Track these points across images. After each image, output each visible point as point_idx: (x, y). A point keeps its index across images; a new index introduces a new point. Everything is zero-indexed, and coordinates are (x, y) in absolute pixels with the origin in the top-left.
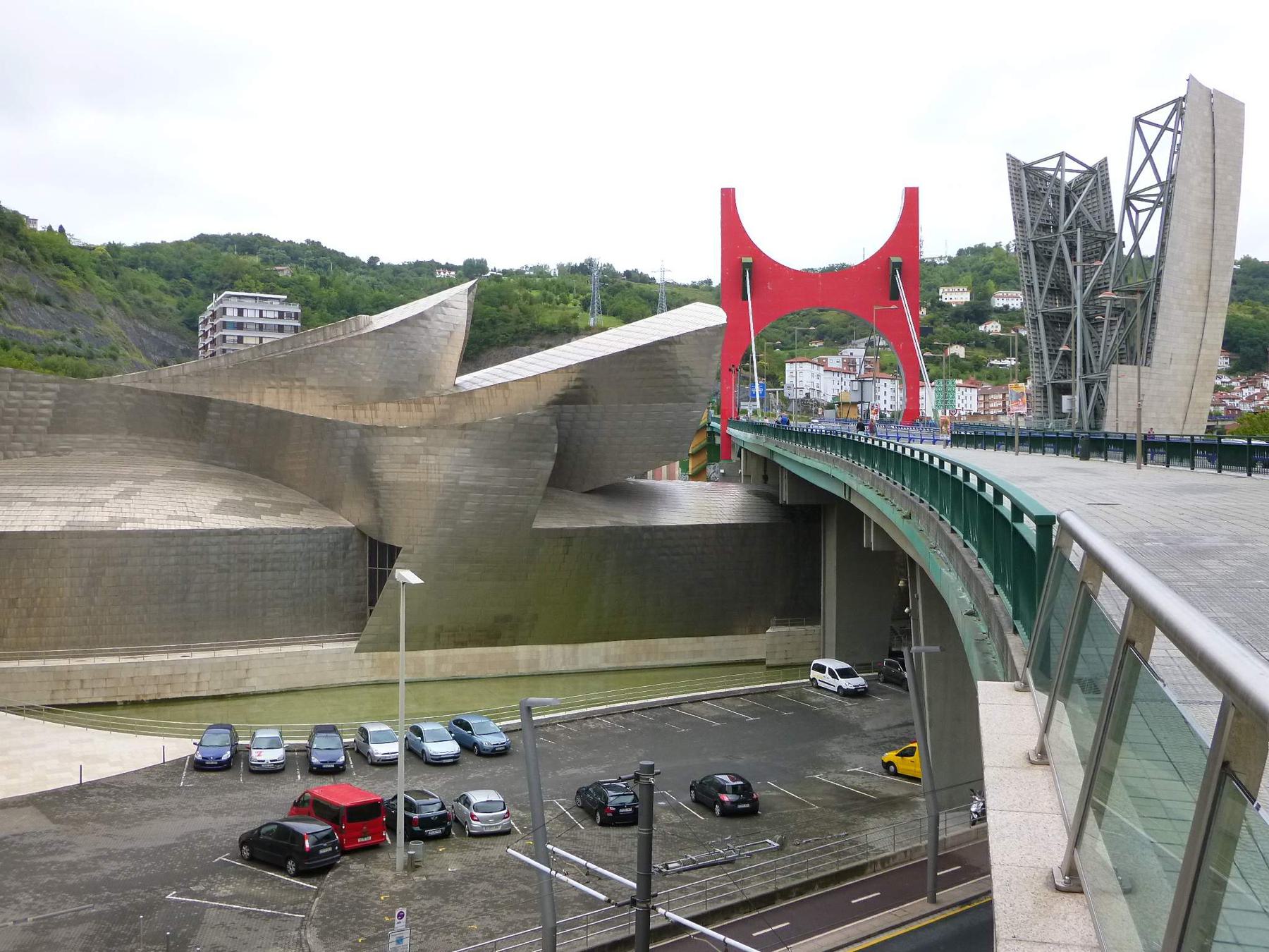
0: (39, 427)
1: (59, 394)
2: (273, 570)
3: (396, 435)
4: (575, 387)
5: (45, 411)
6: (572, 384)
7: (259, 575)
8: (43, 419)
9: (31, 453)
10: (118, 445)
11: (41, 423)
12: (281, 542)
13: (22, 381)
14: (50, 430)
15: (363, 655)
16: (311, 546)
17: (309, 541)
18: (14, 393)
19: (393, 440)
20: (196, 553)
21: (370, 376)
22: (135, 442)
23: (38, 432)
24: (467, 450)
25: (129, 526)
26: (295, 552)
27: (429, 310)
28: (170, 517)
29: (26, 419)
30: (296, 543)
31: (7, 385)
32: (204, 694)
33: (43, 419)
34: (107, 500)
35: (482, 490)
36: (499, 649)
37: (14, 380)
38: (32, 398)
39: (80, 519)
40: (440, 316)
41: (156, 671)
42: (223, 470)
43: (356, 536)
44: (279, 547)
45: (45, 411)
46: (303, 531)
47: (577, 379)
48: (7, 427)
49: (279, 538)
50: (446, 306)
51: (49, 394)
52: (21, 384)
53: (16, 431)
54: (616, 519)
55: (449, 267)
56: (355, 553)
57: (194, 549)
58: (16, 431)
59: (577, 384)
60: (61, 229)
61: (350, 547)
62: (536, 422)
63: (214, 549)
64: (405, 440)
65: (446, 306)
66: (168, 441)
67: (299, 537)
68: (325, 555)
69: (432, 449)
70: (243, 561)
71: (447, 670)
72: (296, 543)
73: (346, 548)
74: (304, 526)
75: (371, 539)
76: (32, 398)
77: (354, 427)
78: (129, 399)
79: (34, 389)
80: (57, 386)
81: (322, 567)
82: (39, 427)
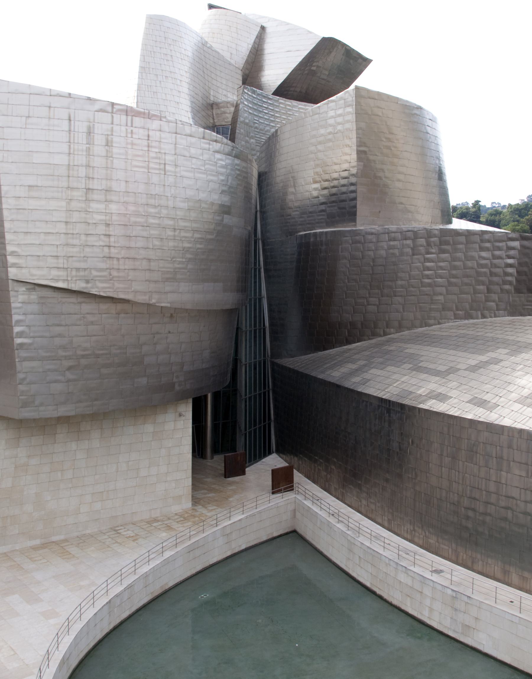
0: (507, 287)
5: (510, 270)
8: (509, 278)
11: (510, 283)
18: (484, 254)
23: (508, 292)
29: (495, 279)
31: (477, 246)
33: (509, 278)
38: (500, 258)
45: (510, 270)
48: (481, 287)
51: (512, 252)
52: (488, 245)
53: (489, 291)
76: (500, 258)
79: (499, 249)
82: (507, 287)
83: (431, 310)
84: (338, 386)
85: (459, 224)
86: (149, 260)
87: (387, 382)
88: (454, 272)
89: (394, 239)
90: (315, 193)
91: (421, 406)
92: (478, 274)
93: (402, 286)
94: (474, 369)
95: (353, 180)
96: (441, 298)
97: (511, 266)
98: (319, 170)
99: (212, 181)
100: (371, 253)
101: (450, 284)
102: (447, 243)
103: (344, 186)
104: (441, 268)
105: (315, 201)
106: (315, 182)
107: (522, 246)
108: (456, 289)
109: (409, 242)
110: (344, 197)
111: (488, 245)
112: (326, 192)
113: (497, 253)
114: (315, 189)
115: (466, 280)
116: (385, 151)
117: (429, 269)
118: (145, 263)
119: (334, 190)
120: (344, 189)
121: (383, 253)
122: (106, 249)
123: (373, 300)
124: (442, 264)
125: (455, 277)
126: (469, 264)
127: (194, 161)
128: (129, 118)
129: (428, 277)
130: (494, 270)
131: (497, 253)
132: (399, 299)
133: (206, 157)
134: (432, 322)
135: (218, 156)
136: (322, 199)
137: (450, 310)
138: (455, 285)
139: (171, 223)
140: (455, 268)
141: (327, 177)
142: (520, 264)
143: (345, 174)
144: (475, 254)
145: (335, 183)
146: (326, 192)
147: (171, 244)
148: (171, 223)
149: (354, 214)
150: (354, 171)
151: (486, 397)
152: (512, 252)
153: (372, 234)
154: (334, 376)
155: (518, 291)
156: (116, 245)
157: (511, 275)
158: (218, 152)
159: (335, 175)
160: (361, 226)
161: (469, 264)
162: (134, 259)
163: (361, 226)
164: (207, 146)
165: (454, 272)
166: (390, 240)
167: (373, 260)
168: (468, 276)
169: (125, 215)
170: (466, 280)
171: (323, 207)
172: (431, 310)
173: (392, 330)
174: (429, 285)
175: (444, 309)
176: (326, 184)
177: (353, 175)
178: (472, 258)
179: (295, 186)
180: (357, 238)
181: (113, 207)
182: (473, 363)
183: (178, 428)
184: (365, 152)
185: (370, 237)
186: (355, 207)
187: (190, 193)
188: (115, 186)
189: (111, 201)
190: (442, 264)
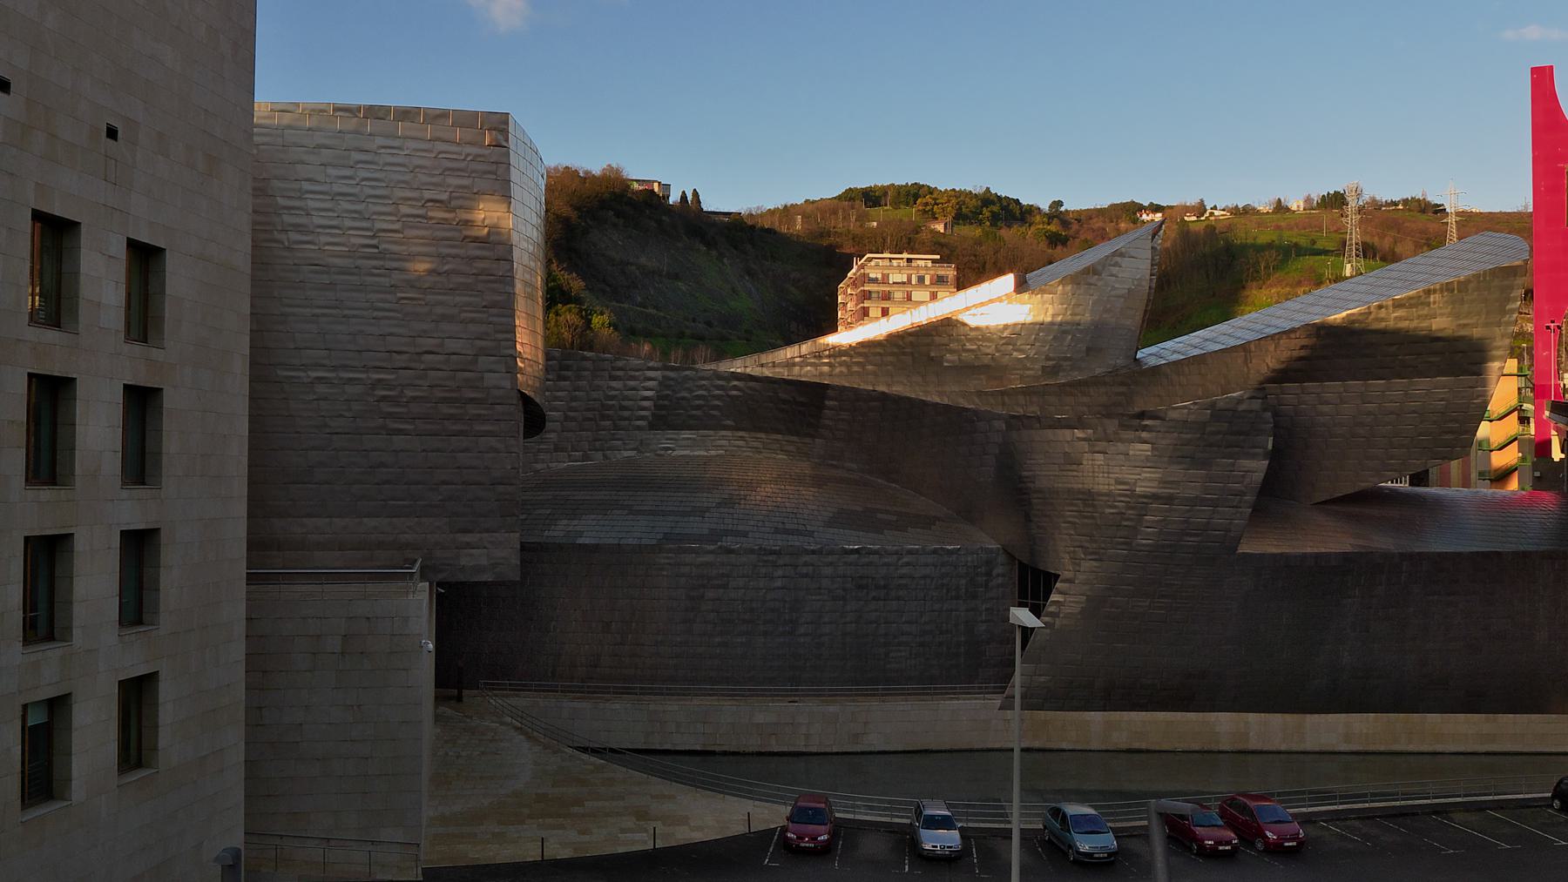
1: (660, 383)
2: (898, 599)
3: (1050, 427)
4: (1301, 359)
6: (1296, 354)
12: (908, 564)
14: (652, 427)
17: (943, 565)
18: (614, 384)
19: (1049, 434)
20: (806, 575)
21: (1021, 351)
22: (742, 438)
23: (639, 428)
24: (1148, 446)
26: (924, 577)
27: (1099, 262)
28: (777, 531)
29: (626, 414)
30: (926, 565)
31: (606, 374)
32: (814, 749)
34: (708, 509)
35: (1169, 500)
36: (1192, 716)
37: (614, 369)
39: (677, 531)
40: (1115, 270)
43: (1002, 558)
44: (904, 571)
47: (1302, 347)
50: (1122, 255)
54: (1361, 542)
55: (1156, 208)
56: (1000, 580)
57: (805, 570)
58: (617, 428)
59: (1303, 353)
60: (695, 193)
61: (995, 573)
62: (1242, 407)
63: (828, 571)
64: (1067, 434)
65: (1122, 255)
66: (779, 437)
67: (930, 559)
68: (963, 582)
69: (1102, 445)
70: (860, 587)
71: (1120, 740)
72: (926, 565)
73: (989, 574)
75: (1020, 563)
77: (999, 417)
78: (735, 388)
81: (957, 598)
83: (539, 451)
96: (553, 435)
102: (567, 368)
104: (557, 398)
113: (632, 383)
115: (589, 414)
126: (595, 395)
131: (632, 383)
138: (573, 419)
161: (595, 395)
168: (588, 410)
170: (589, 414)
172: (539, 451)
175: (556, 450)
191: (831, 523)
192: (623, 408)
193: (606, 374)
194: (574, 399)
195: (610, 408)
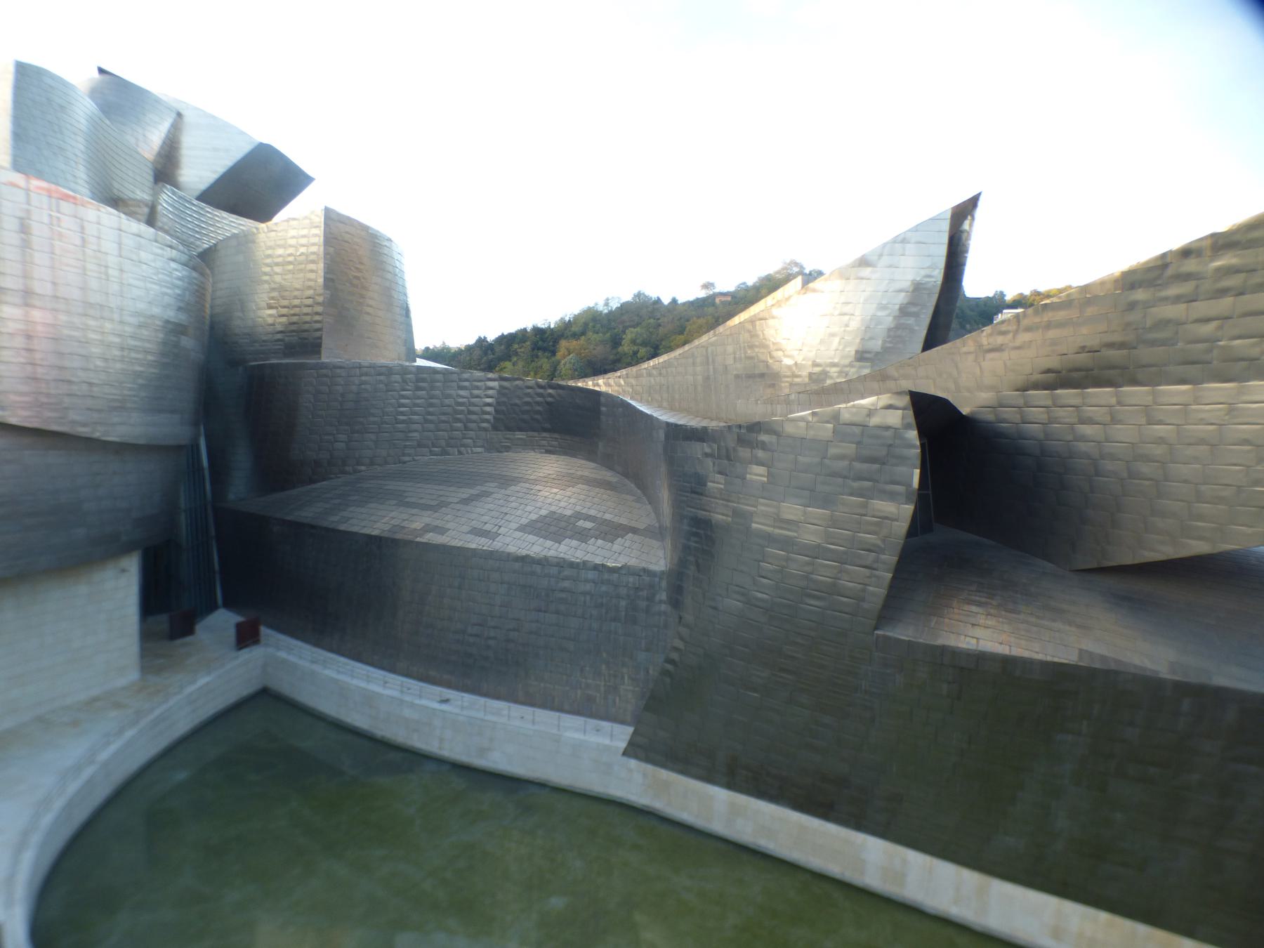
0: (485, 425)
1: (499, 392)
2: (557, 612)
5: (488, 409)
7: (542, 614)
9: (479, 450)
10: (544, 442)
11: (487, 421)
13: (467, 380)
15: (633, 763)
16: (604, 588)
18: (462, 393)
23: (485, 429)
25: (430, 538)
29: (473, 417)
36: (832, 828)
37: (461, 380)
38: (477, 397)
41: (407, 713)
42: (608, 475)
44: (566, 584)
45: (488, 409)
46: (596, 567)
48: (459, 425)
49: (567, 572)
51: (490, 392)
52: (466, 384)
53: (466, 428)
61: (657, 598)
67: (591, 575)
68: (623, 603)
72: (587, 581)
74: (598, 561)
76: (477, 397)
78: (550, 395)
79: (478, 388)
80: (495, 384)
82: (485, 425)
83: (406, 447)
84: (313, 527)
85: (421, 362)
86: (91, 384)
87: (375, 520)
88: (431, 409)
89: (366, 374)
90: (270, 321)
91: (418, 539)
92: (456, 412)
93: (374, 423)
94: (466, 501)
95: (319, 309)
96: (415, 434)
97: (489, 405)
98: (275, 294)
99: (166, 294)
100: (339, 388)
101: (426, 421)
103: (307, 314)
105: (270, 329)
106: (270, 307)
107: (501, 387)
108: (431, 426)
109: (382, 378)
110: (306, 326)
111: (466, 384)
112: (284, 320)
113: (476, 392)
114: (270, 316)
116: (355, 282)
117: (403, 406)
118: (85, 387)
119: (295, 319)
120: (308, 318)
121: (354, 388)
122: (29, 368)
123: (342, 437)
124: (418, 401)
125: (430, 414)
127: (144, 267)
128: (54, 201)
129: (402, 413)
130: (472, 408)
131: (476, 392)
132: (373, 436)
133: (159, 264)
134: (407, 459)
135: (173, 265)
136: (279, 328)
137: (425, 446)
138: (431, 422)
139: (117, 340)
140: (432, 405)
141: (285, 303)
142: (498, 403)
143: (310, 302)
144: (452, 392)
145: (297, 310)
146: (284, 320)
147: (119, 366)
148: (117, 340)
149: (320, 346)
150: (320, 299)
151: (488, 527)
152: (490, 392)
153: (341, 368)
154: (307, 514)
155: (495, 428)
156: (45, 363)
157: (488, 413)
158: (173, 260)
159: (296, 302)
160: (325, 358)
161: (447, 401)
162: (70, 382)
163: (325, 358)
164: (159, 251)
165: (431, 409)
166: (361, 375)
167: (342, 395)
168: (444, 414)
169: (53, 326)
170: (443, 418)
171: (279, 336)
173: (363, 468)
174: (403, 422)
175: (420, 445)
176: (285, 311)
177: (318, 304)
178: (448, 396)
179: (243, 311)
180: (324, 371)
181: (37, 315)
182: (465, 496)
183: (119, 588)
184: (332, 280)
185: (338, 371)
186: (320, 338)
187: (141, 306)
188: (37, 287)
189: (34, 307)
190: (418, 401)
191: (522, 528)
192: (470, 412)
193: (454, 384)
194: (432, 405)
195: (461, 412)
